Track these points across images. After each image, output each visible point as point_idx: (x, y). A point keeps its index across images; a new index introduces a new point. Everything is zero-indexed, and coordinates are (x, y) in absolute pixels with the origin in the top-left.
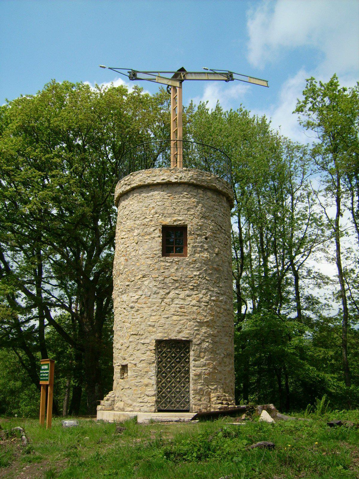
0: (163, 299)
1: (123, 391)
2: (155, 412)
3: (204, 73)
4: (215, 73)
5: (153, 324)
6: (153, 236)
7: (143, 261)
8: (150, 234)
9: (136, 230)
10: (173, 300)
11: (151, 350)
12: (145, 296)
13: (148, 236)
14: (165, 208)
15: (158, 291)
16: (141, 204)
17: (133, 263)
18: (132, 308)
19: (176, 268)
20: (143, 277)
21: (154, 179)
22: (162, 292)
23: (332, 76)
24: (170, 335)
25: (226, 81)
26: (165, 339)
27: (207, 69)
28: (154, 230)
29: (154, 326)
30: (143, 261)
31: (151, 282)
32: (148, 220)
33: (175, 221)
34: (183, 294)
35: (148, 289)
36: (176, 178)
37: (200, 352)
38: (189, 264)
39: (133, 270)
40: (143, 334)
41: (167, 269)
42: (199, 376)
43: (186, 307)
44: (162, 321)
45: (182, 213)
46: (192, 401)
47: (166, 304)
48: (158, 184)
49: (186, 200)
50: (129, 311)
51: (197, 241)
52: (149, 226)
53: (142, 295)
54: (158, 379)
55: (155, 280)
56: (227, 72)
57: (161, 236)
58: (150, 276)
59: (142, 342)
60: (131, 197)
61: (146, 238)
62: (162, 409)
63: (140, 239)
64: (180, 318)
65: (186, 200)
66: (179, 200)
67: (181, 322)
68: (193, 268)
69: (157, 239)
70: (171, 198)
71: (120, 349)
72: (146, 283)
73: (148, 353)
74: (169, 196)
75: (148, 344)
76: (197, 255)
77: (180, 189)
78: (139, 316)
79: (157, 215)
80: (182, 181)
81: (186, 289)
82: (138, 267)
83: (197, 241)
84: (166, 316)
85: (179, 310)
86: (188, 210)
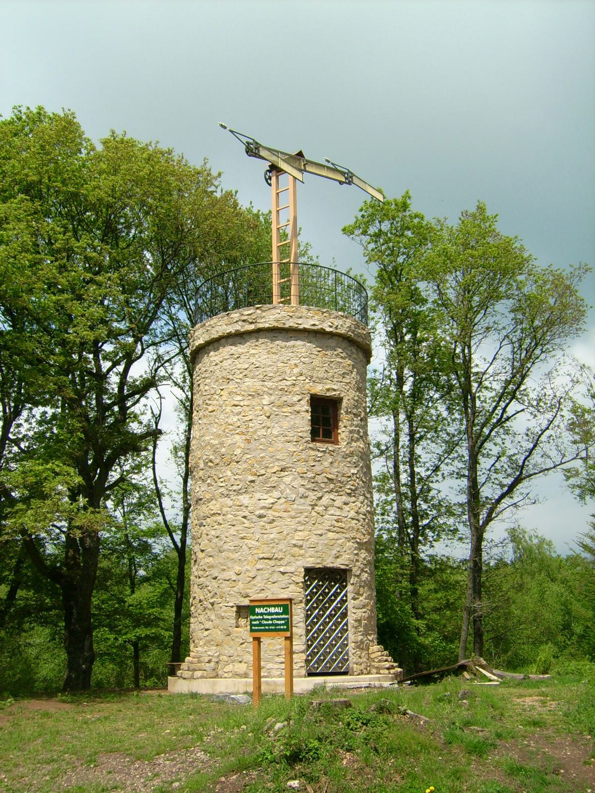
0: (313, 506)
1: (244, 646)
2: (305, 677)
3: (324, 166)
4: (335, 170)
5: (301, 543)
6: (297, 408)
7: (280, 445)
8: (292, 405)
9: (265, 396)
10: (326, 508)
11: (297, 583)
12: (284, 500)
13: (289, 408)
14: (314, 369)
15: (306, 494)
16: (274, 356)
17: (261, 447)
18: (261, 516)
19: (330, 460)
20: (281, 471)
21: (300, 321)
22: (313, 496)
23: (403, 194)
24: (325, 561)
25: (341, 183)
26: (318, 566)
27: (329, 162)
28: (299, 401)
29: (301, 547)
30: (280, 445)
31: (295, 479)
32: (289, 383)
33: (328, 390)
34: (339, 501)
35: (290, 489)
36: (331, 327)
37: (360, 586)
38: (346, 456)
39: (262, 457)
40: (282, 559)
41: (319, 461)
42: (358, 621)
43: (344, 519)
44: (314, 539)
45: (336, 379)
46: (353, 659)
47: (318, 513)
48: (305, 330)
49: (340, 360)
50: (254, 521)
51: (355, 423)
52: (290, 392)
53: (279, 499)
54: (307, 626)
55: (302, 477)
56: (347, 171)
57: (310, 410)
58: (294, 470)
59: (282, 569)
60: (252, 343)
61: (284, 410)
62: (314, 672)
63: (275, 411)
64: (337, 536)
65: (340, 360)
66: (333, 360)
67: (340, 542)
68: (350, 462)
69: (304, 414)
70: (320, 354)
71: (234, 581)
72: (287, 480)
73: (292, 587)
74: (319, 351)
75: (292, 573)
76: (354, 444)
77: (332, 342)
78: (275, 530)
79: (303, 378)
80: (338, 331)
81: (342, 493)
82: (273, 454)
83: (355, 423)
84: (319, 532)
85: (336, 524)
86: (343, 375)
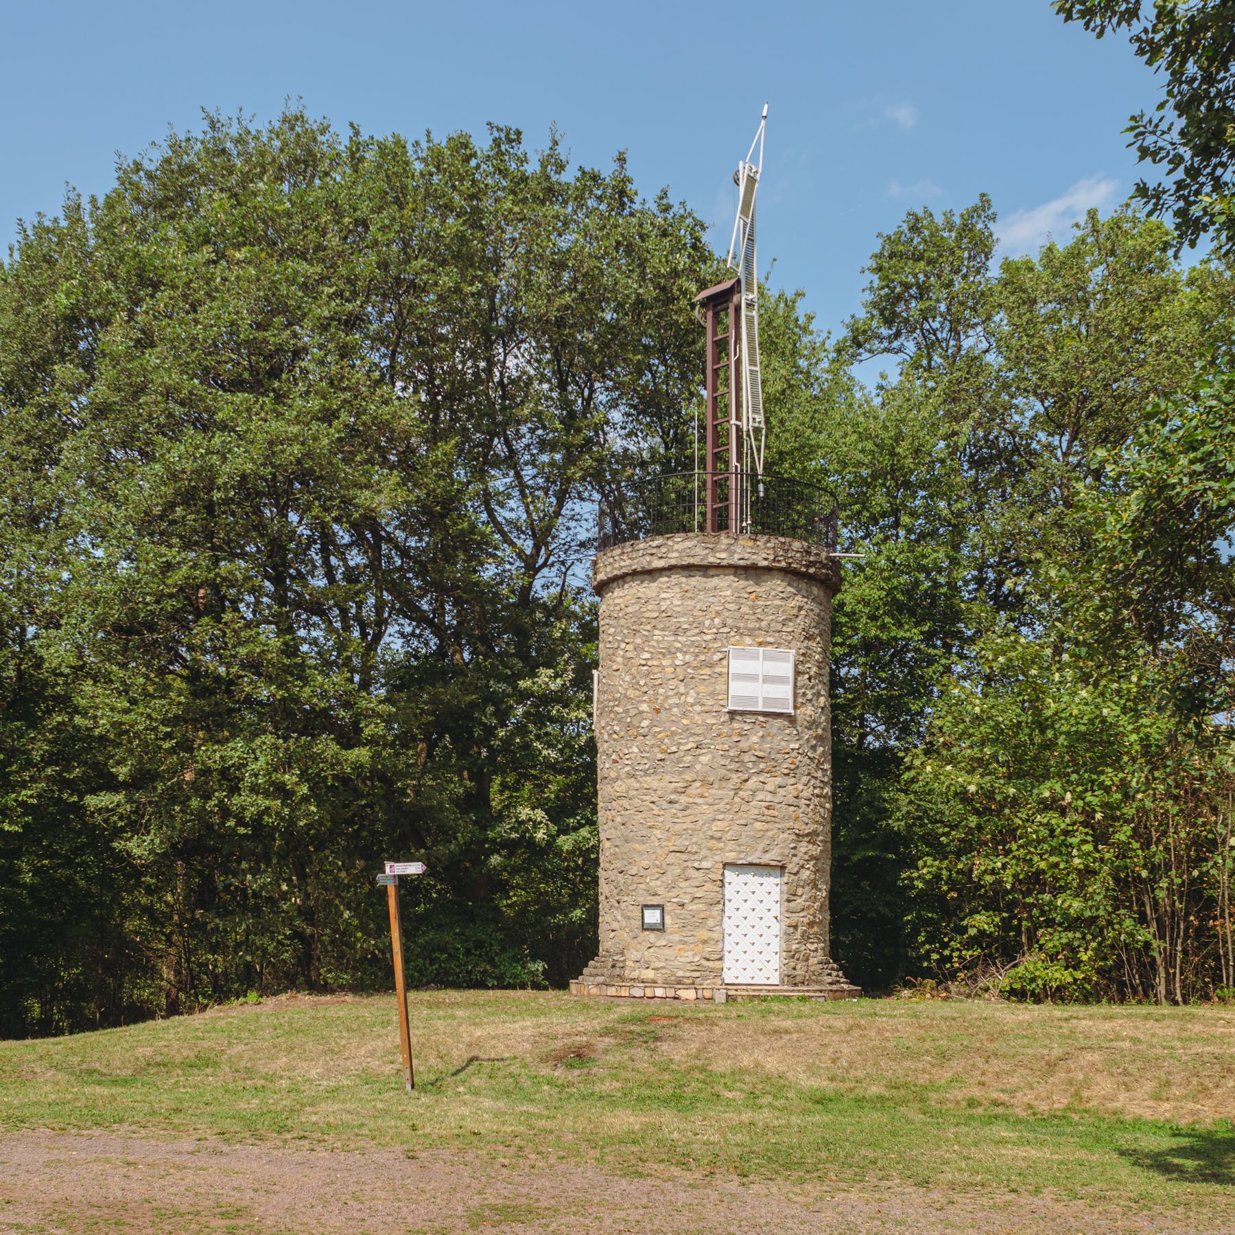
5: (719, 835)
19: (761, 734)
34: (772, 783)
37: (798, 886)
49: (780, 603)
59: (696, 865)
64: (766, 826)
65: (780, 603)
67: (770, 834)
78: (689, 819)
79: (726, 630)
85: (766, 812)
